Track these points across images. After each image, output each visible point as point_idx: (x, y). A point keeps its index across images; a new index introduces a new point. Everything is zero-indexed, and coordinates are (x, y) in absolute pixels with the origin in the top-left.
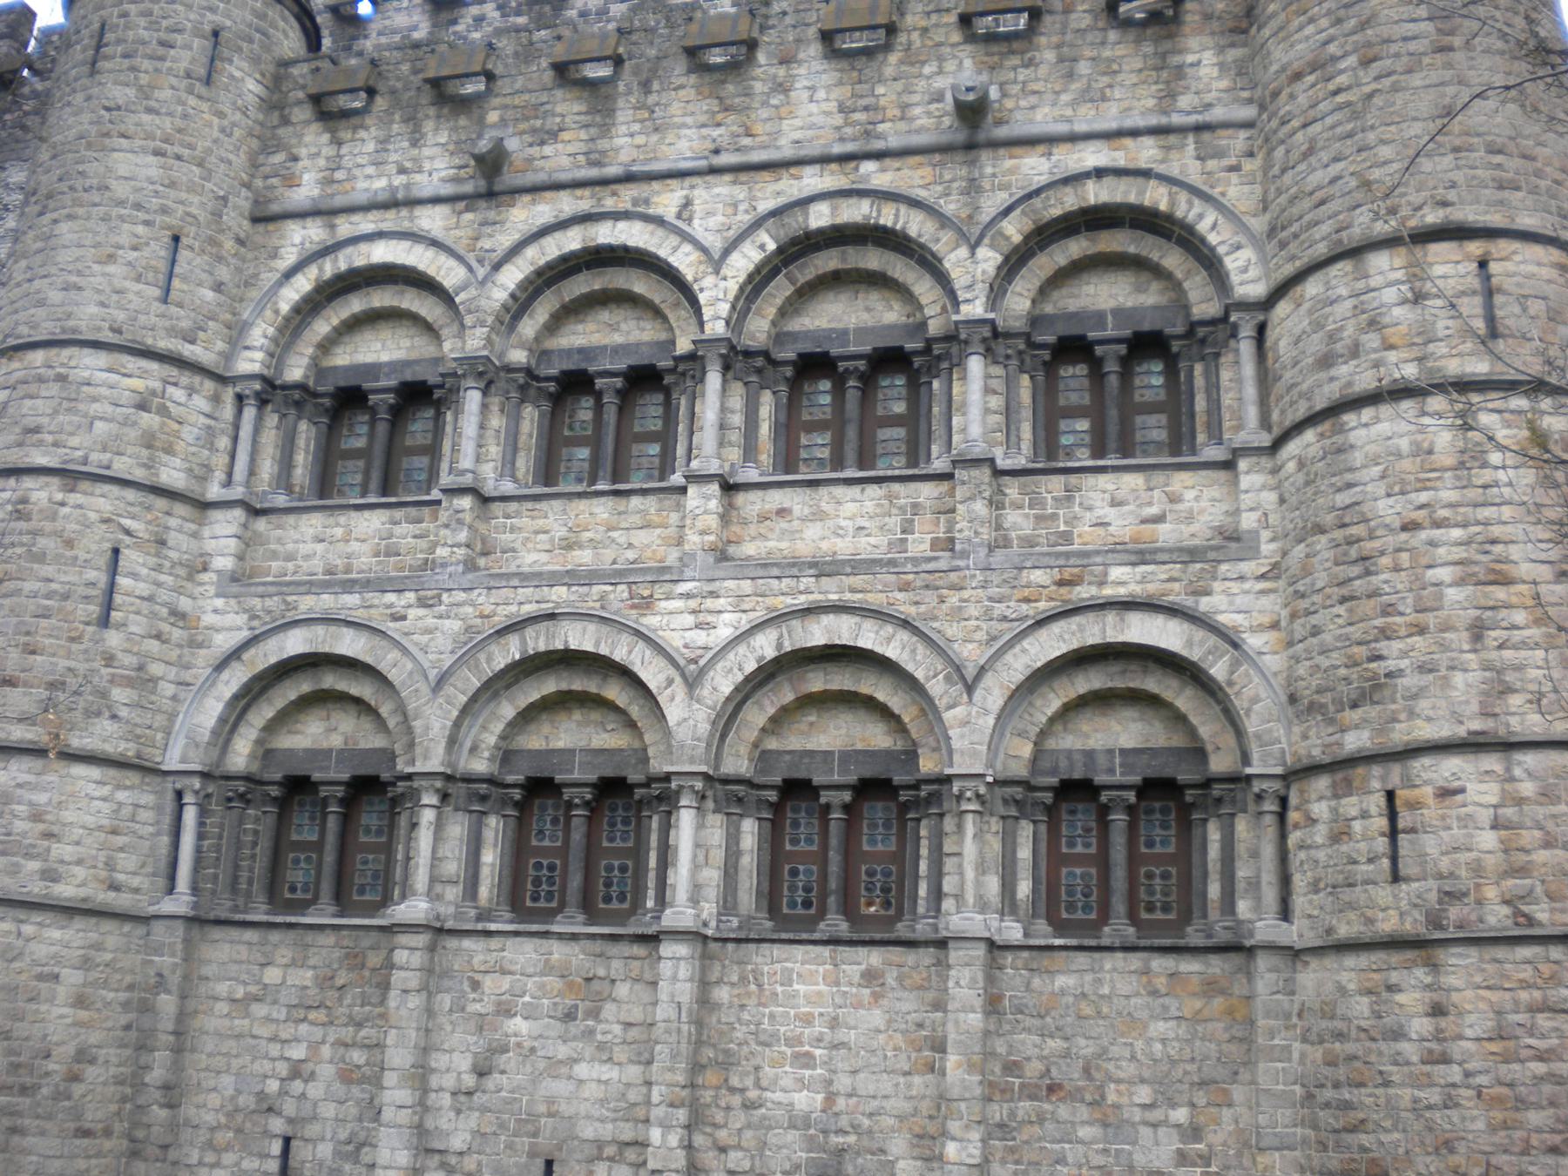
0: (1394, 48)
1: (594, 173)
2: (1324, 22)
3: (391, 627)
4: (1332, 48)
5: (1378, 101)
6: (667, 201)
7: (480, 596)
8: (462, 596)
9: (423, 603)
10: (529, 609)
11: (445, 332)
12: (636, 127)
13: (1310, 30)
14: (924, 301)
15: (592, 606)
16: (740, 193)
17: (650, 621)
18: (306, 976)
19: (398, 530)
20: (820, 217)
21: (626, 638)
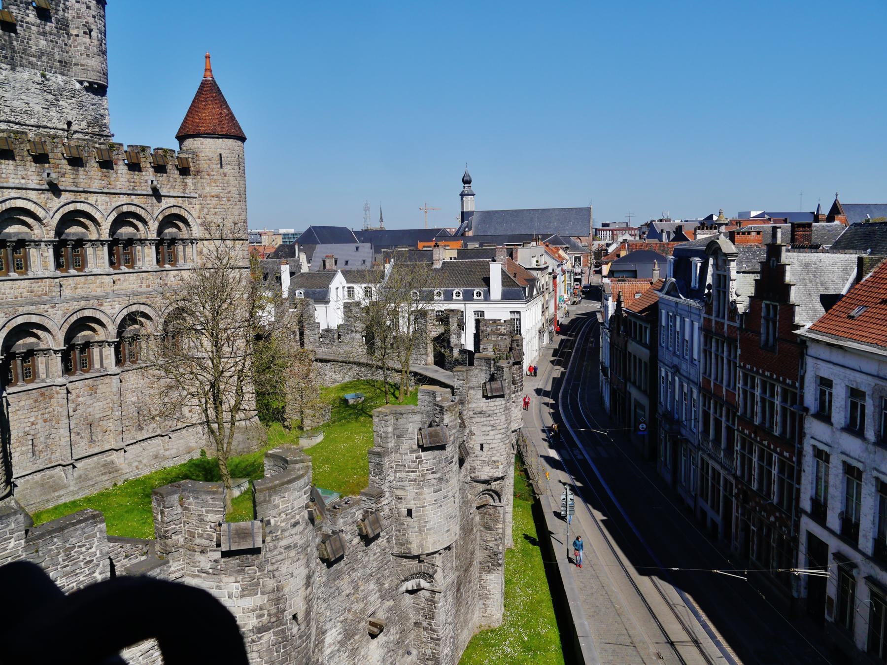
0: (233, 199)
1: (76, 189)
2: (220, 188)
3: (45, 314)
4: (221, 195)
5: (230, 210)
6: (92, 199)
7: (65, 304)
8: (61, 305)
9: (53, 307)
10: (78, 307)
11: (34, 228)
12: (84, 177)
13: (216, 188)
14: (140, 229)
15: (90, 306)
16: (107, 199)
17: (102, 308)
18: (31, 401)
19: (33, 285)
20: (125, 209)
21: (98, 312)
